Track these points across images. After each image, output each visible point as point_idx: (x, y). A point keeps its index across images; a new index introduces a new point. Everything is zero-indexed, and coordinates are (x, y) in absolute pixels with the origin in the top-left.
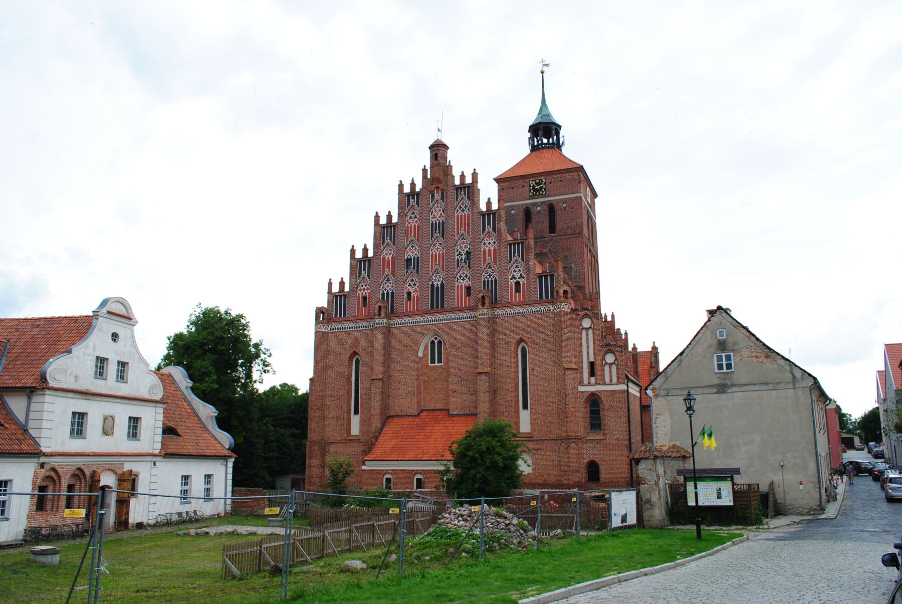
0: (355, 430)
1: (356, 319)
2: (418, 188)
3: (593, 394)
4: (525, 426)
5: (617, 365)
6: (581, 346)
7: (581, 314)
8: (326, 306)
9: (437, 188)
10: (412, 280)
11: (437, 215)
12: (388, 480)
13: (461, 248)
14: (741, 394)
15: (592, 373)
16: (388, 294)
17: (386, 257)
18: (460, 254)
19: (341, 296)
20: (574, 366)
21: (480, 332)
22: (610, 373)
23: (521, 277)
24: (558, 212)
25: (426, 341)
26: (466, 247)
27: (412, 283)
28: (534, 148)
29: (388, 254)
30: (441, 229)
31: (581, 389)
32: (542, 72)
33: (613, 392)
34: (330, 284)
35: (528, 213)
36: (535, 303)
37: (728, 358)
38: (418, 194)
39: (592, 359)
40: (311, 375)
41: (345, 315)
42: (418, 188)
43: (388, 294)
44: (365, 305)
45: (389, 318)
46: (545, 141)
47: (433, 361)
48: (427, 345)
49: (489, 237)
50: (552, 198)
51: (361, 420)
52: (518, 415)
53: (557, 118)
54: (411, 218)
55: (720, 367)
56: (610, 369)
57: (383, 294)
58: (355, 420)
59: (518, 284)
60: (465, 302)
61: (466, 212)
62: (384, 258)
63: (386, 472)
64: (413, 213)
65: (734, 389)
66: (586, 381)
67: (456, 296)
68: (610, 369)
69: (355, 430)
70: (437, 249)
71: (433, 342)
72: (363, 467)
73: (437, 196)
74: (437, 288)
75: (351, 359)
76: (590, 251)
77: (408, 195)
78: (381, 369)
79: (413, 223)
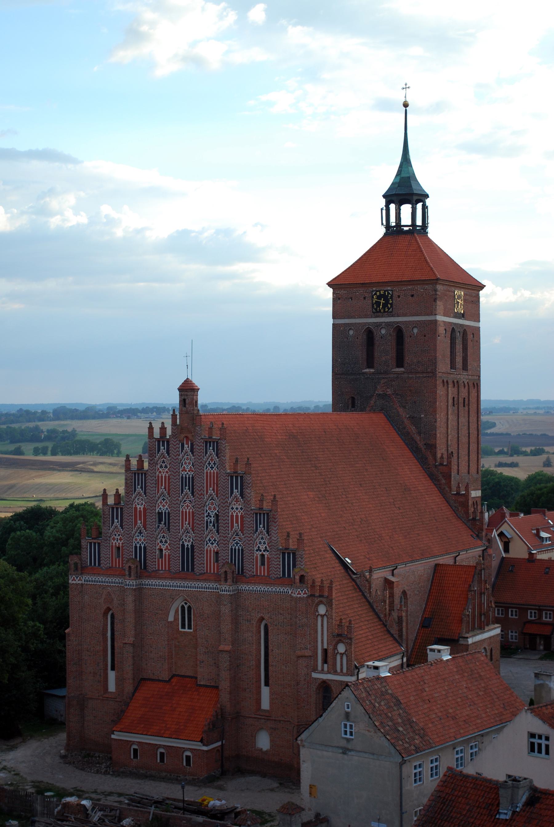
0: (112, 687)
1: (111, 571)
2: (169, 432)
3: (324, 682)
4: (265, 705)
5: (347, 657)
6: (317, 632)
7: (317, 600)
9: (187, 437)
10: (164, 537)
12: (135, 751)
13: (210, 509)
15: (325, 661)
16: (140, 547)
17: (138, 507)
18: (209, 515)
22: (341, 663)
24: (407, 340)
25: (177, 604)
26: (215, 509)
27: (164, 540)
30: (190, 483)
31: (314, 675)
35: (370, 335)
37: (351, 727)
39: (325, 647)
41: (99, 564)
43: (140, 547)
44: (119, 556)
47: (183, 626)
48: (178, 608)
49: (237, 501)
51: (117, 678)
52: (259, 693)
54: (161, 467)
56: (342, 659)
57: (136, 547)
59: (263, 556)
60: (213, 568)
61: (215, 470)
62: (136, 508)
64: (164, 462)
65: (352, 753)
66: (320, 668)
67: (204, 562)
68: (342, 659)
69: (112, 687)
70: (188, 506)
71: (183, 607)
72: (113, 736)
74: (188, 549)
77: (158, 441)
78: (133, 632)
79: (164, 473)
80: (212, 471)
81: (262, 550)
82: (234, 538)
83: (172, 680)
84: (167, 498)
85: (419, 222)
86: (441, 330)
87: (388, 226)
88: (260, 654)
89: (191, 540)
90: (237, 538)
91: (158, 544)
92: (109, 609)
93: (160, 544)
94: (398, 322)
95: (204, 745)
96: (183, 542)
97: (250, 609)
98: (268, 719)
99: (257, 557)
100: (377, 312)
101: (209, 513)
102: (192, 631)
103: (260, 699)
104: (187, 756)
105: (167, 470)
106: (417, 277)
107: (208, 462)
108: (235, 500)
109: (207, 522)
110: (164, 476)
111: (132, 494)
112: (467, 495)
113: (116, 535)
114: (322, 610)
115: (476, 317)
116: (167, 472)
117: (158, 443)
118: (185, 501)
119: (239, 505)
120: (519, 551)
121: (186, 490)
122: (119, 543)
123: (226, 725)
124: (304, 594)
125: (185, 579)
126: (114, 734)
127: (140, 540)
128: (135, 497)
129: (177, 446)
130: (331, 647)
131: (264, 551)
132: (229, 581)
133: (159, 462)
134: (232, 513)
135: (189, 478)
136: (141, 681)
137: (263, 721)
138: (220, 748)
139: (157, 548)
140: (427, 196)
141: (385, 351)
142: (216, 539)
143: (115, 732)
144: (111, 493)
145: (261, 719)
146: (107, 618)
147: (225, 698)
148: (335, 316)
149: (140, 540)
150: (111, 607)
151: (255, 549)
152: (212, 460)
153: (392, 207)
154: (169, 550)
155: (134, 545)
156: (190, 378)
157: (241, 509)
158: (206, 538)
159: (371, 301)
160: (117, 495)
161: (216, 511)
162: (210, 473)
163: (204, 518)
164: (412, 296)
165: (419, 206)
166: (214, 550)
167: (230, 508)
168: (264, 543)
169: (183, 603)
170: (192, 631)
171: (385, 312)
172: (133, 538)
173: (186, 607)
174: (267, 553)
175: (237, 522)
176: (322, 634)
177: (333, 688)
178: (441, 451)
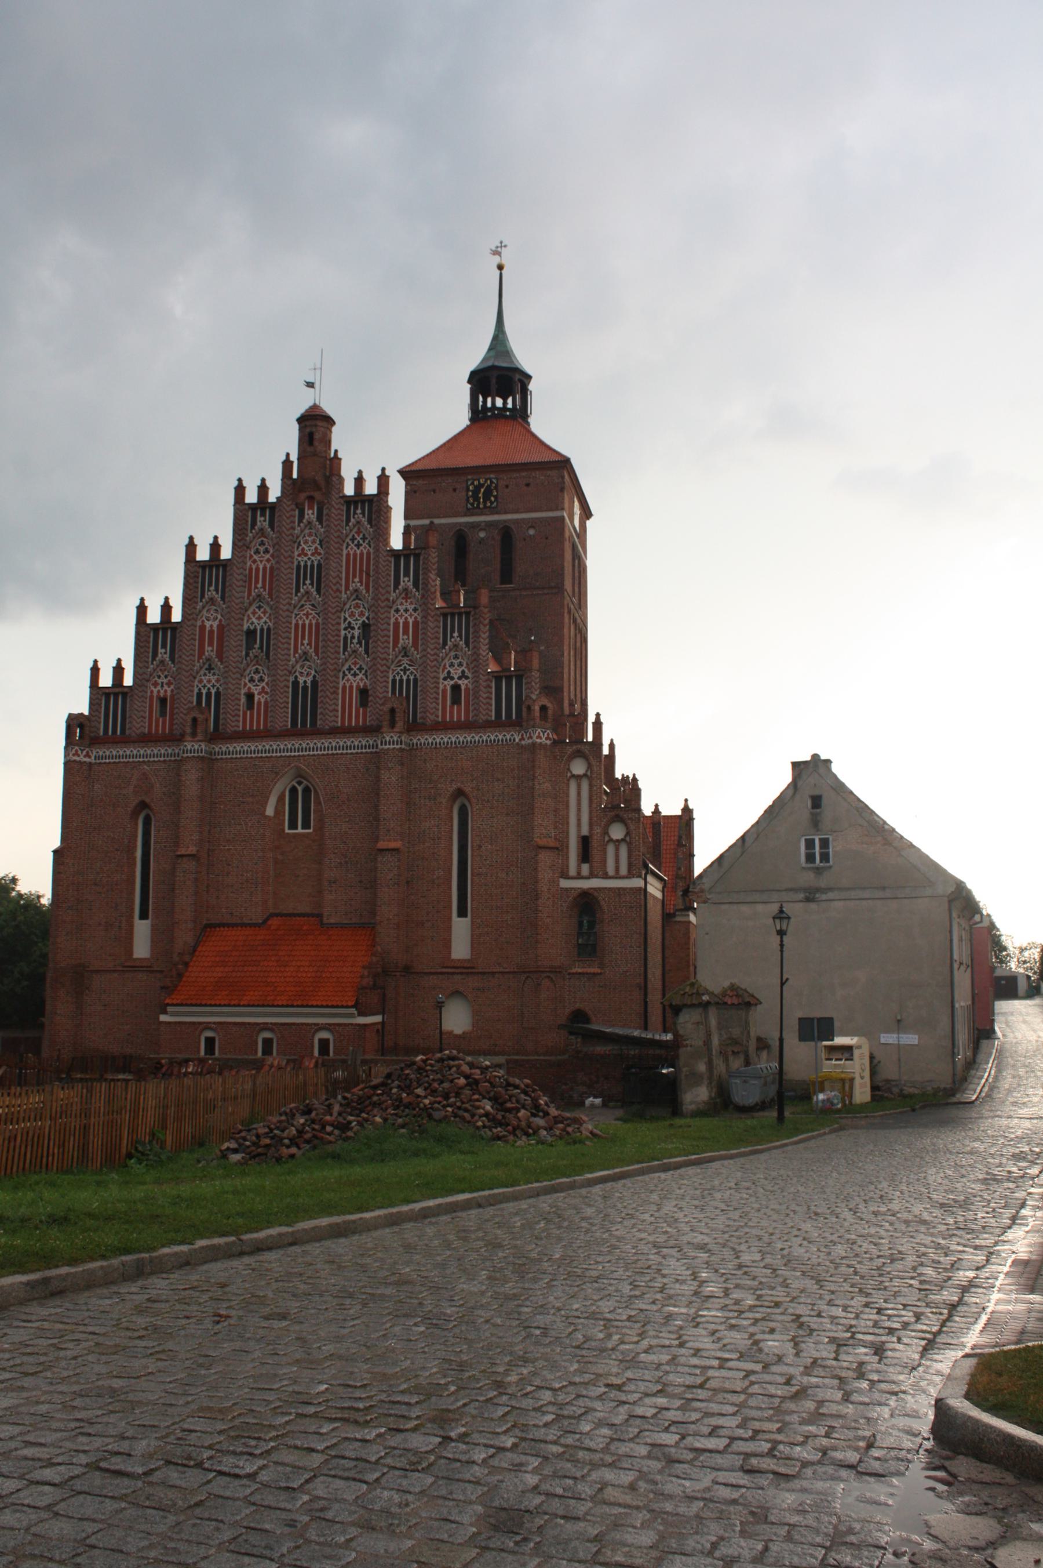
2: (273, 496)
4: (461, 949)
5: (629, 844)
6: (567, 806)
8: (86, 713)
9: (311, 498)
10: (257, 671)
11: (308, 551)
14: (841, 903)
15: (585, 856)
16: (209, 694)
17: (208, 624)
18: (350, 626)
19: (116, 695)
20: (552, 843)
21: (385, 775)
23: (463, 676)
26: (362, 614)
28: (478, 415)
31: (564, 883)
32: (500, 267)
33: (620, 892)
34: (95, 671)
35: (461, 541)
36: (488, 725)
37: (825, 843)
38: (273, 507)
39: (585, 831)
40: (57, 843)
42: (274, 494)
43: (209, 694)
46: (499, 402)
47: (293, 825)
50: (509, 517)
51: (154, 929)
52: (449, 929)
53: (525, 357)
54: (257, 552)
55: (810, 858)
56: (617, 850)
57: (200, 695)
58: (142, 929)
59: (456, 688)
61: (364, 548)
62: (203, 627)
63: (207, 1026)
64: (262, 544)
65: (831, 895)
66: (572, 872)
67: (337, 709)
68: (617, 850)
70: (307, 615)
71: (293, 791)
72: (163, 1018)
73: (310, 514)
74: (305, 688)
75: (135, 814)
76: (575, 621)
79: (262, 562)
80: (358, 552)
81: (456, 677)
82: (400, 661)
83: (270, 922)
84: (268, 603)
88: (451, 859)
89: (313, 672)
90: (405, 661)
91: (245, 685)
92: (143, 805)
93: (249, 685)
94: (505, 521)
95: (361, 1014)
96: (296, 677)
97: (435, 778)
98: (467, 973)
99: (444, 691)
100: (474, 508)
101: (350, 623)
102: (311, 831)
103: (450, 941)
104: (321, 1041)
105: (268, 556)
107: (350, 537)
108: (403, 595)
109: (346, 638)
110: (261, 567)
111: (196, 603)
113: (159, 677)
116: (268, 560)
118: (303, 606)
119: (411, 603)
121: (308, 586)
122: (166, 691)
124: (547, 739)
126: (165, 1012)
127: (209, 681)
128: (204, 607)
129: (292, 513)
130: (598, 830)
131: (460, 678)
132: (400, 725)
133: (253, 544)
134: (397, 619)
135: (312, 566)
137: (459, 977)
138: (380, 1027)
139: (243, 691)
140: (529, 377)
142: (364, 666)
143: (169, 1009)
145: (453, 973)
146: (137, 824)
149: (209, 681)
150: (147, 800)
151: (442, 676)
152: (358, 533)
154: (267, 693)
155: (196, 690)
156: (317, 403)
157: (415, 610)
158: (343, 665)
159: (464, 494)
161: (364, 619)
162: (355, 555)
163: (339, 631)
164: (528, 485)
166: (358, 686)
167: (392, 612)
168: (460, 665)
169: (294, 783)
170: (311, 831)
171: (485, 507)
172: (195, 678)
173: (300, 789)
174: (466, 682)
175: (406, 632)
176: (579, 810)
177: (602, 903)
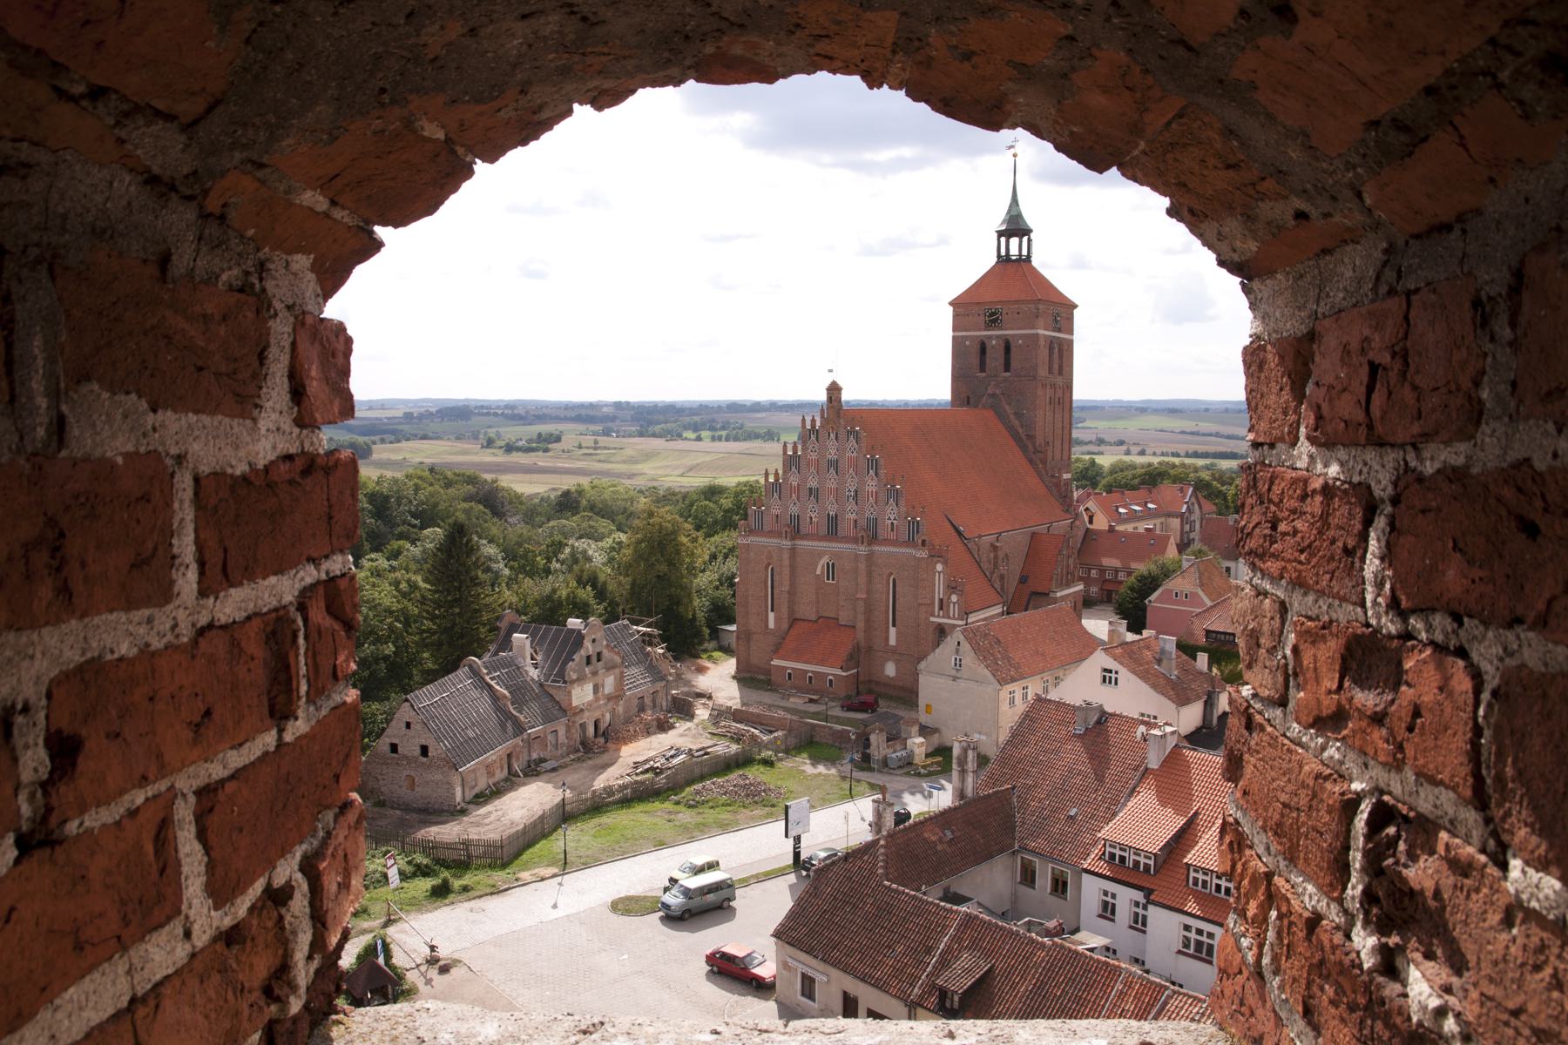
0: (771, 625)
1: (771, 534)
2: (818, 424)
4: (892, 641)
22: (954, 610)
24: (1013, 349)
29: (794, 481)
30: (834, 465)
45: (793, 539)
67: (845, 528)
69: (771, 625)
73: (832, 436)
79: (814, 456)
85: (1025, 252)
86: (1042, 342)
87: (999, 256)
106: (1023, 297)
112: (1059, 477)
114: (939, 567)
115: (1071, 332)
117: (809, 434)
120: (1101, 523)
123: (858, 656)
125: (830, 540)
136: (794, 621)
141: (995, 359)
144: (772, 471)
147: (860, 635)
148: (955, 329)
153: (1003, 240)
160: (776, 474)
165: (1025, 239)
178: (1039, 441)
